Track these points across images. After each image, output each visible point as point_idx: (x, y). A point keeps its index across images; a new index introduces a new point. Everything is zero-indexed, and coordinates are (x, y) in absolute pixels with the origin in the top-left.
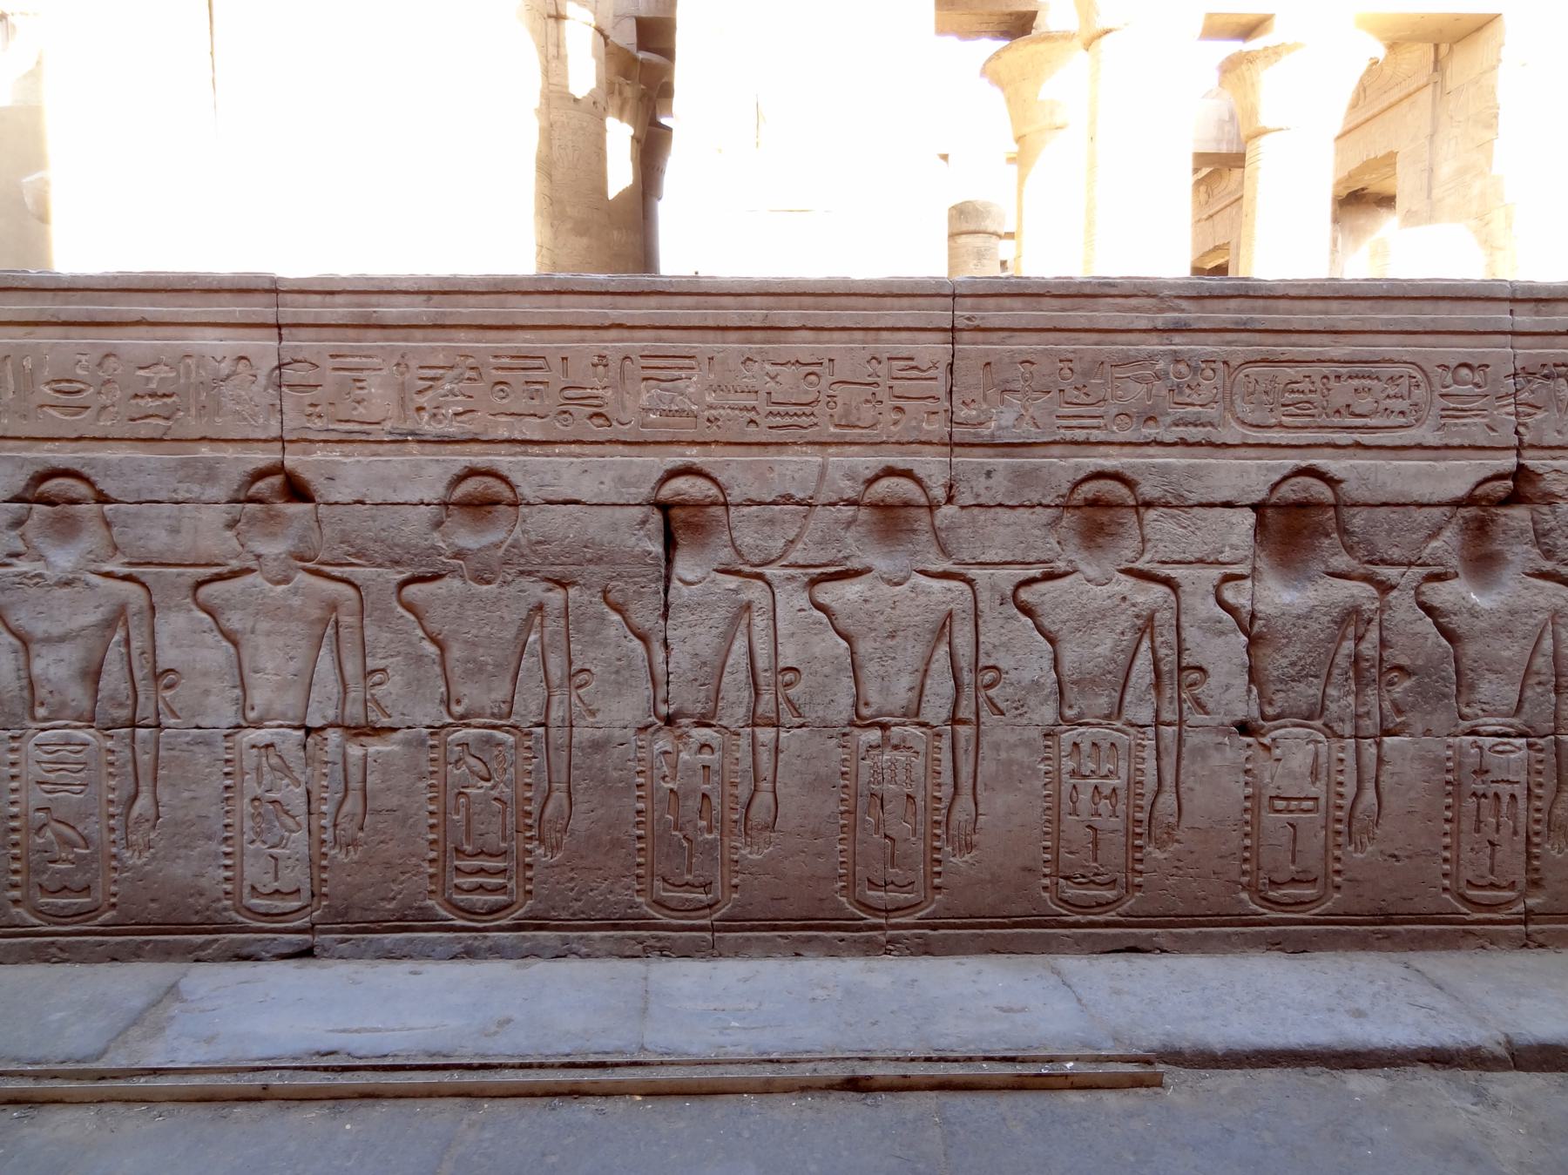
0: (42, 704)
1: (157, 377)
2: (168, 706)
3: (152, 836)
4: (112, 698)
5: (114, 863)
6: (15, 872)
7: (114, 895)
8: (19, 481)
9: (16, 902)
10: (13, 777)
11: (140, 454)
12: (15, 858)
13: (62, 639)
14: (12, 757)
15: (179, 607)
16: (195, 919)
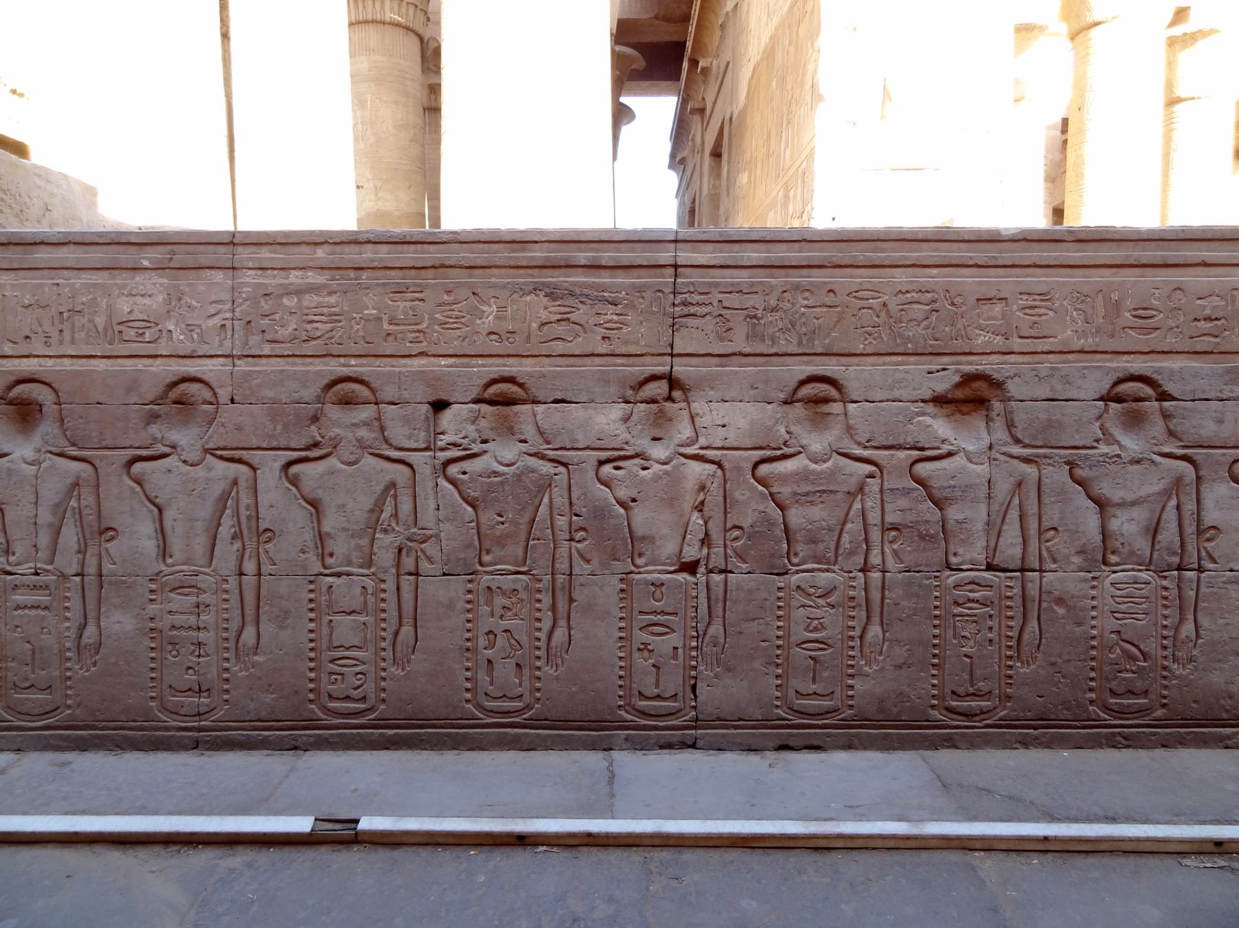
0: (1113, 553)
1: (1208, 306)
2: (1208, 552)
3: (1194, 652)
4: (1168, 549)
5: (1165, 673)
6: (1092, 679)
7: (1165, 697)
8: (1105, 386)
9: (1092, 702)
10: (1094, 608)
11: (1195, 364)
12: (1092, 669)
13: (1133, 504)
14: (1093, 592)
15: (1222, 479)
16: (1225, 716)
